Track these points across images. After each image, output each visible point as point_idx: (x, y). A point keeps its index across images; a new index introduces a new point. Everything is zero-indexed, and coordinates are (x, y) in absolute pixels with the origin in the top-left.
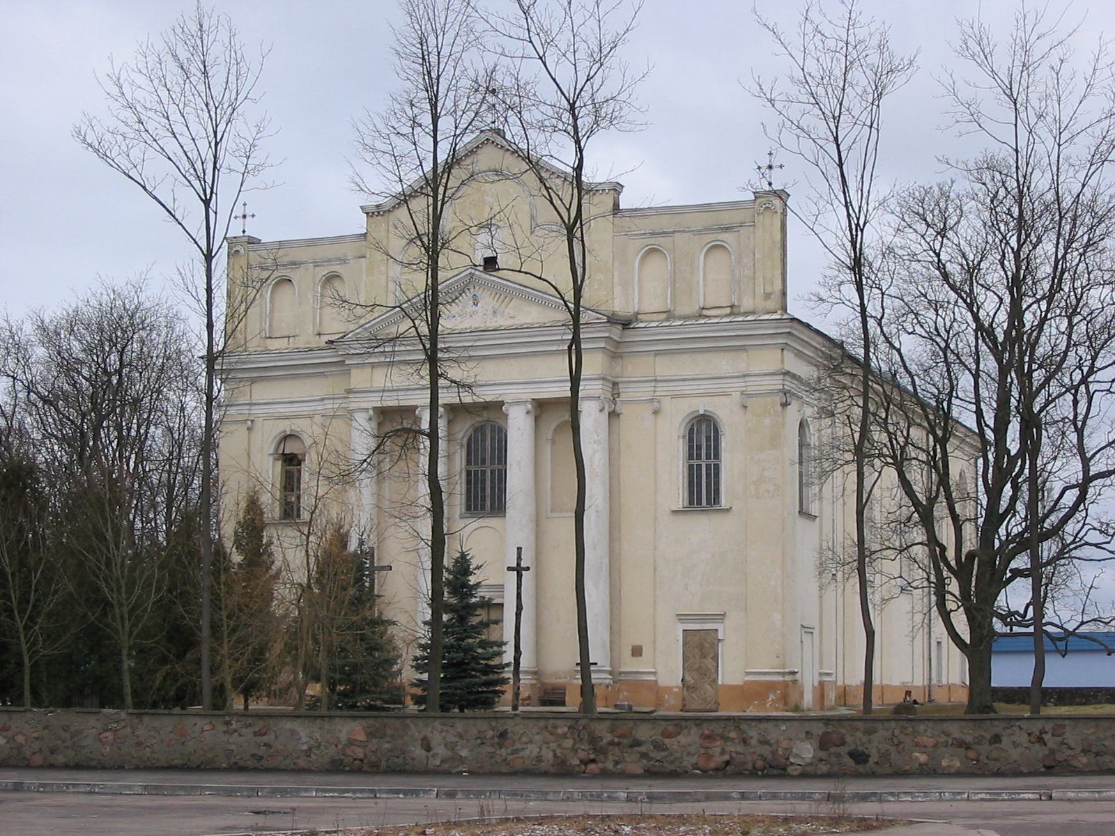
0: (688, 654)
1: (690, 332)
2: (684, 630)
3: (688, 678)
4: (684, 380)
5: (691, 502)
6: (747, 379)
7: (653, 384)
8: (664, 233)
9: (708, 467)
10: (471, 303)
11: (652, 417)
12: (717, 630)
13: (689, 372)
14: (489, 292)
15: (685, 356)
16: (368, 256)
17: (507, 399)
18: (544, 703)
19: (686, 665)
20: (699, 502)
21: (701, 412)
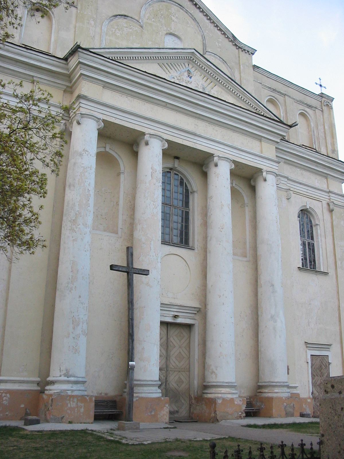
0: (314, 374)
1: (308, 155)
2: (311, 355)
3: (315, 392)
4: (300, 184)
5: (303, 266)
6: (331, 194)
7: (286, 180)
8: (281, 93)
9: (309, 244)
10: (186, 74)
11: (286, 201)
12: (328, 356)
13: (304, 181)
14: (199, 73)
15: (298, 170)
16: (79, 7)
17: (216, 153)
18: (248, 414)
19: (314, 381)
20: (307, 267)
21: (308, 208)
